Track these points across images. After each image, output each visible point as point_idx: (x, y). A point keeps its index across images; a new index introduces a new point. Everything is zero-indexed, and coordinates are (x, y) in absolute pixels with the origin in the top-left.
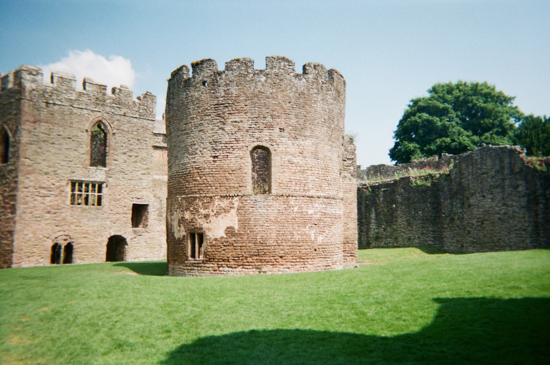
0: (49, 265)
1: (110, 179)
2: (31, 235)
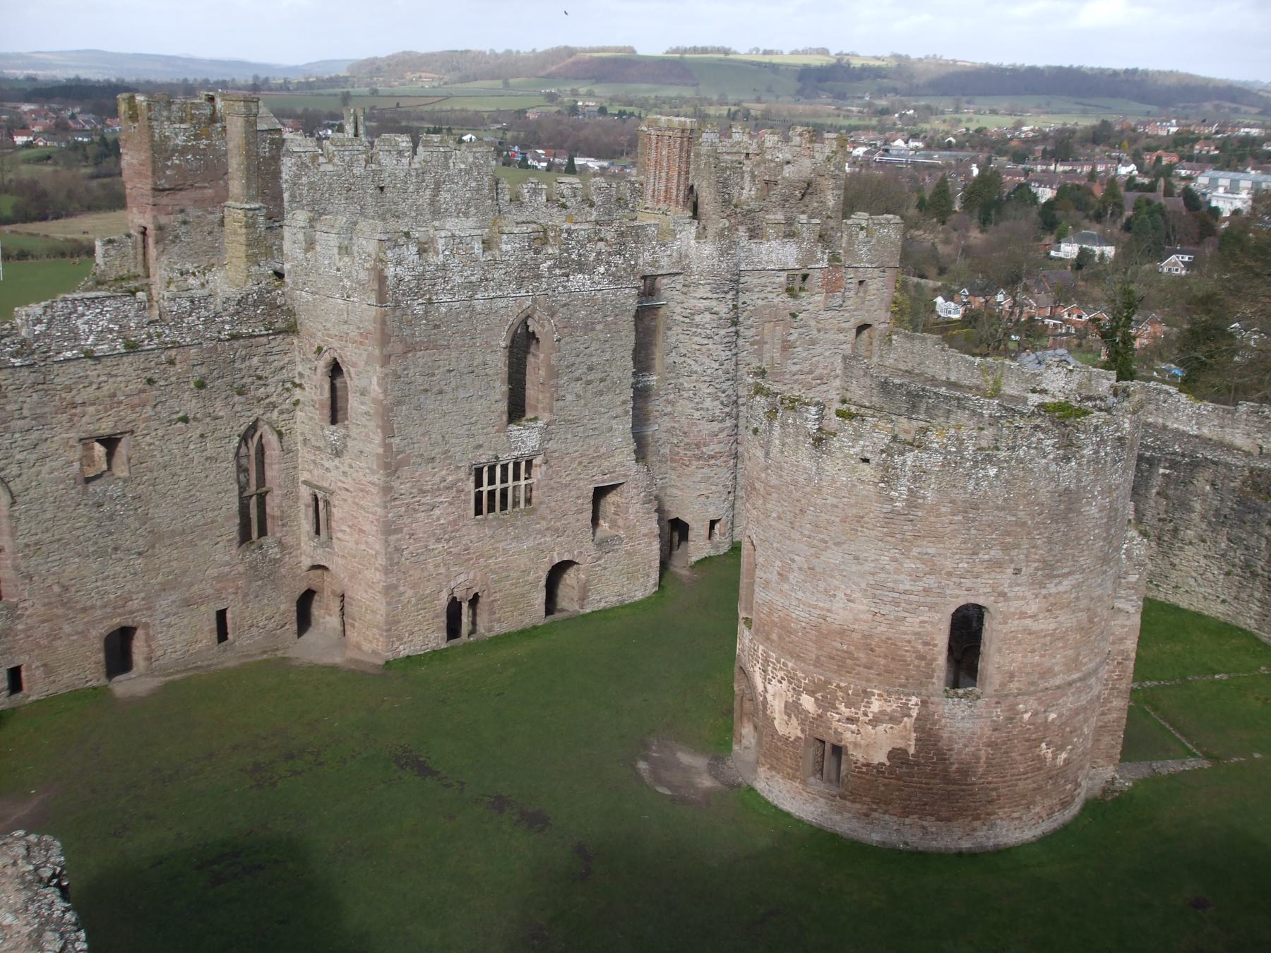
0: (444, 646)
1: (551, 445)
2: (410, 593)
